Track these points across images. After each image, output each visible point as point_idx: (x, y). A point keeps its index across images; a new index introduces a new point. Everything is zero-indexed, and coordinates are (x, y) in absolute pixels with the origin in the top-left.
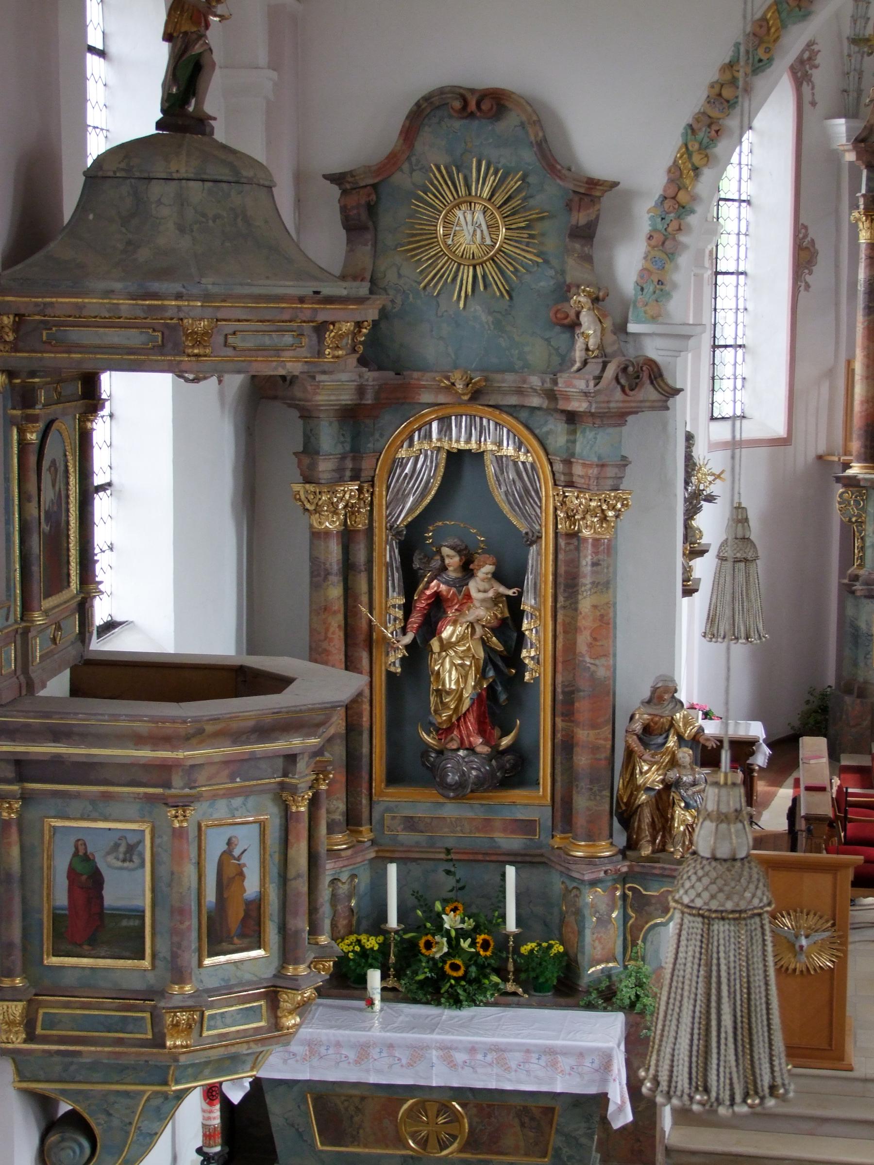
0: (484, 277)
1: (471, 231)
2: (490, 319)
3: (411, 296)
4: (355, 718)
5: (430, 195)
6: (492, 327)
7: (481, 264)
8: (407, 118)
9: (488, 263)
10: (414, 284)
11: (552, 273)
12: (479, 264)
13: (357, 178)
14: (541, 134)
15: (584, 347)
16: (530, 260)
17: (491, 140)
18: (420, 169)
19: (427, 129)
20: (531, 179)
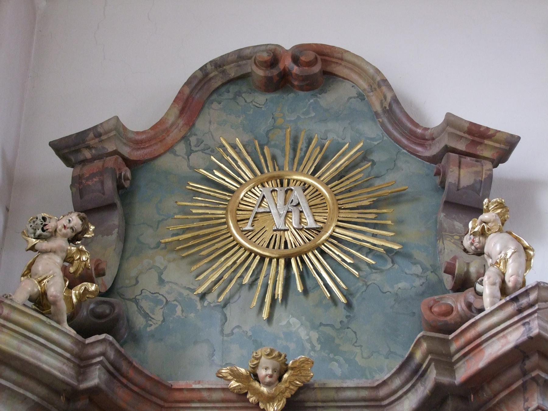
0: (304, 275)
1: (283, 212)
2: (315, 335)
3: (179, 309)
5: (217, 173)
6: (318, 347)
7: (299, 255)
8: (187, 83)
9: (310, 255)
10: (185, 293)
11: (417, 269)
12: (295, 255)
13: (104, 137)
14: (389, 96)
15: (498, 280)
16: (382, 246)
17: (313, 114)
18: (203, 151)
19: (215, 105)
20: (375, 157)
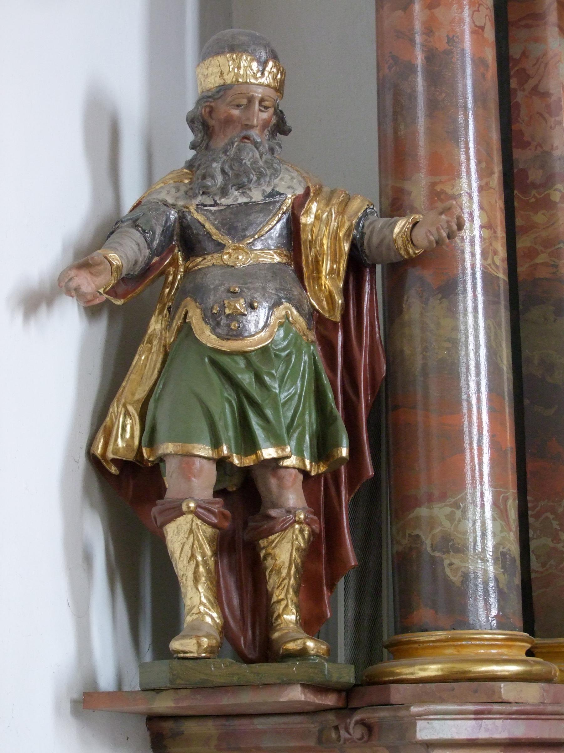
4: (542, 258)
